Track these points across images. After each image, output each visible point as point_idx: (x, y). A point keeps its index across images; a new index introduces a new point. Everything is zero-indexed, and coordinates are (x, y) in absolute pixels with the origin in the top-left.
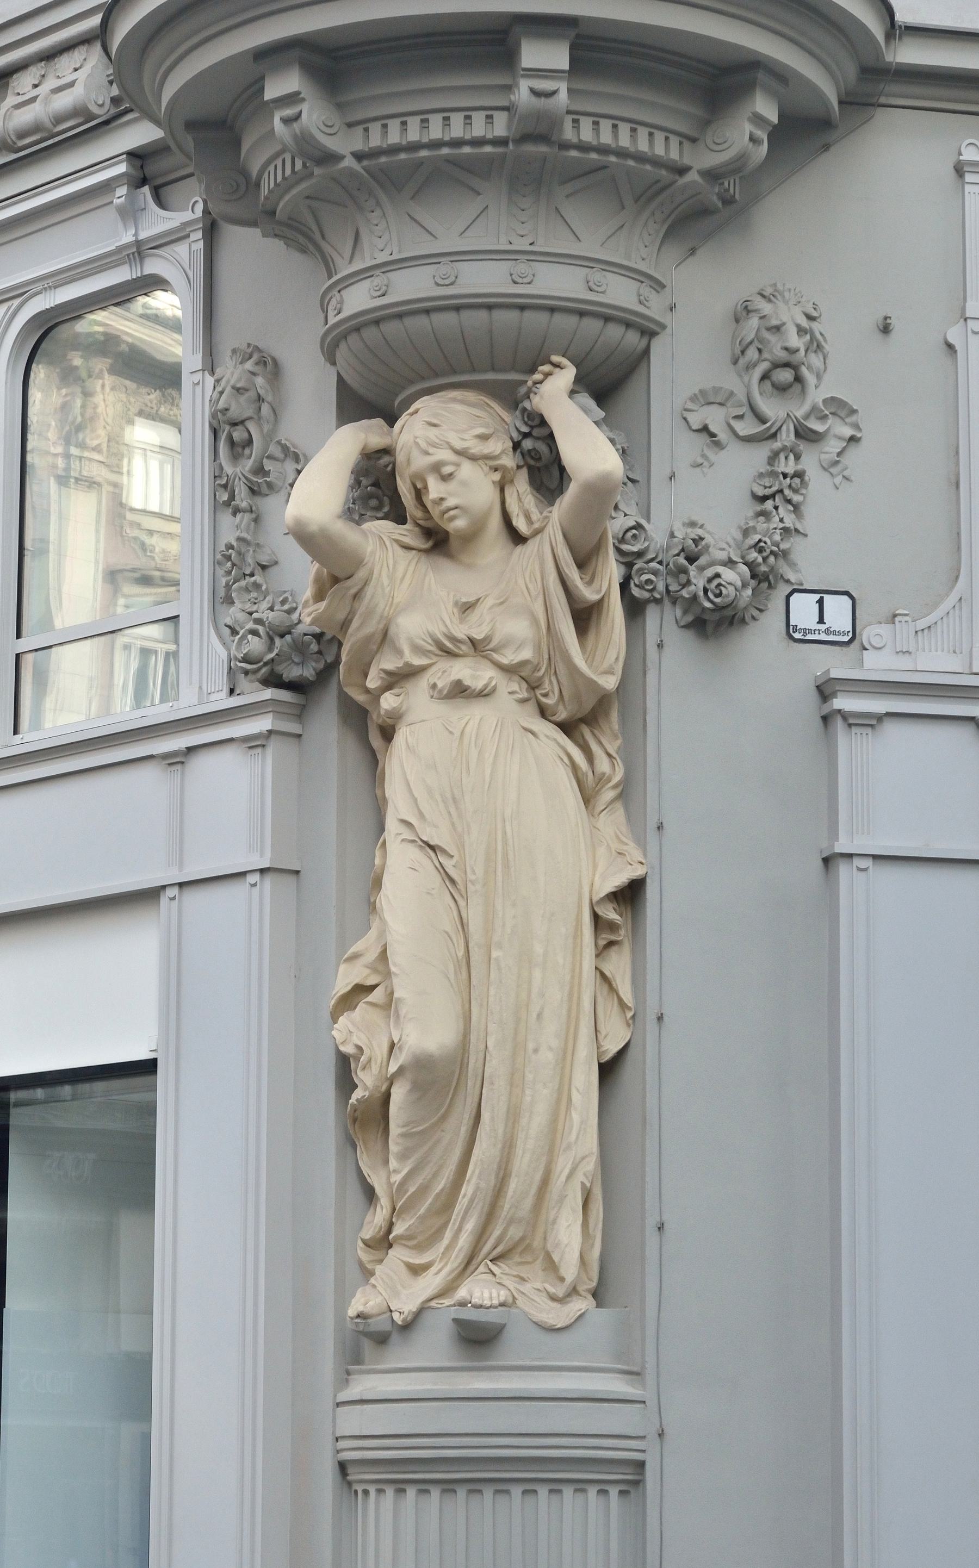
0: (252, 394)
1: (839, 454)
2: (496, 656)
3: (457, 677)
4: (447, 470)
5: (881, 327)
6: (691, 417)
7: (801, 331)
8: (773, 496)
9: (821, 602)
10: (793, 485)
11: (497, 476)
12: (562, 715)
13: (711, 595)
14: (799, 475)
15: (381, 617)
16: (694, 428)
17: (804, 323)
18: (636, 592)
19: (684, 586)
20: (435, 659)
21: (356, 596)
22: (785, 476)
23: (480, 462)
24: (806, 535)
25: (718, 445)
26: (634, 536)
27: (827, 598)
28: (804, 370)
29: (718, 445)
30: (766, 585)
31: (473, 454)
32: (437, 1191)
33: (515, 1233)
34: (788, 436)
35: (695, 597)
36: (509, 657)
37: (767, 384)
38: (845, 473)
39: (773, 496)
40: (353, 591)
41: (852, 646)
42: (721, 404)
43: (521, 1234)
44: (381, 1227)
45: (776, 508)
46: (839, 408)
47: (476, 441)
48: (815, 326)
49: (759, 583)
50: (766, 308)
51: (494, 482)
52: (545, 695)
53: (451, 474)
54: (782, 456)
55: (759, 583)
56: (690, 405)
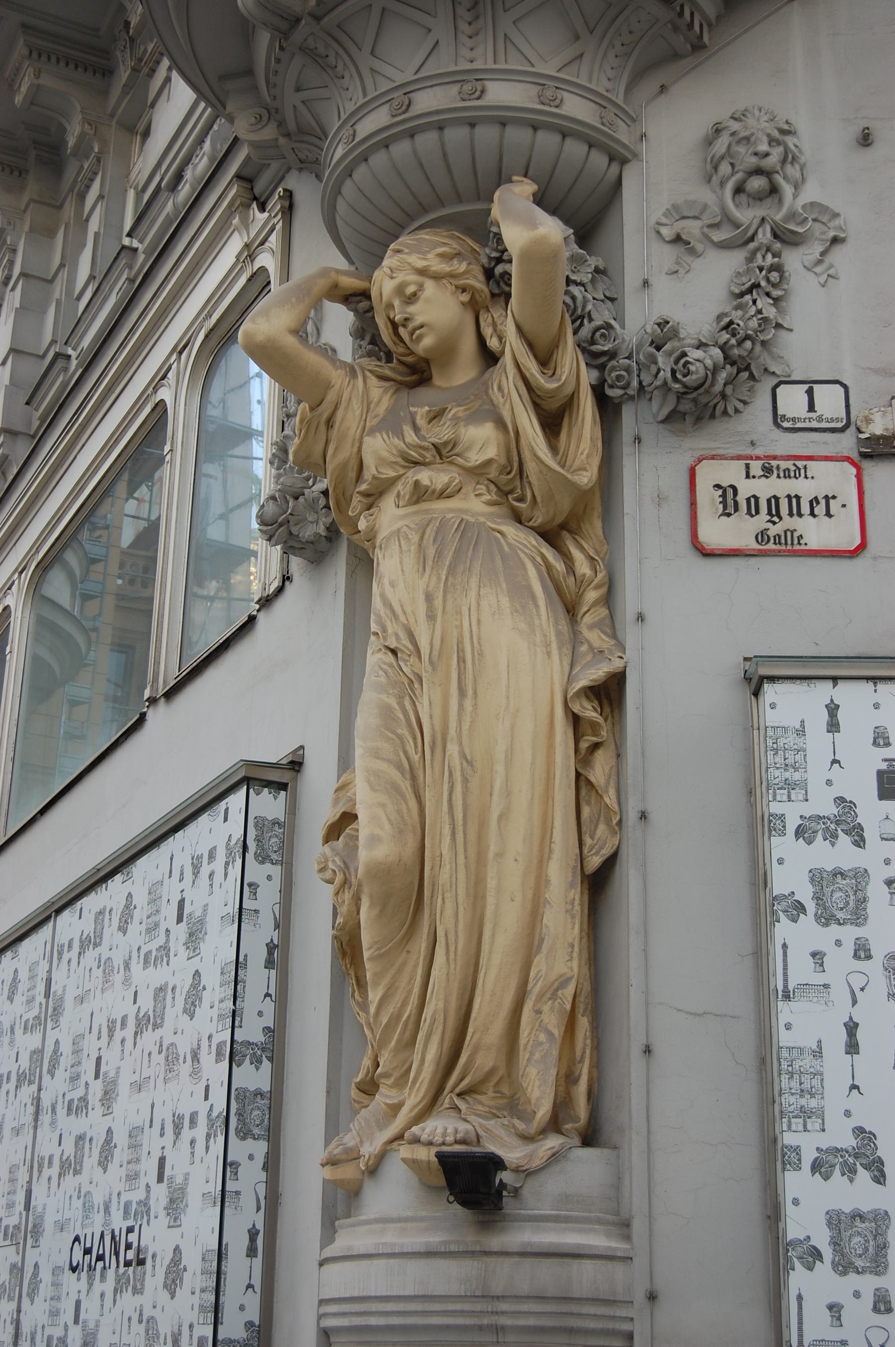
1: (823, 254)
2: (459, 460)
3: (414, 479)
4: (411, 289)
5: (861, 141)
6: (665, 231)
7: (772, 141)
8: (750, 291)
9: (810, 393)
10: (772, 279)
11: (465, 297)
12: (539, 519)
13: (679, 376)
14: (777, 268)
15: (354, 440)
16: (667, 239)
17: (776, 134)
18: (610, 392)
20: (402, 472)
21: (329, 423)
22: (761, 269)
23: (444, 281)
24: (791, 330)
25: (692, 252)
26: (603, 335)
27: (816, 387)
28: (779, 179)
29: (692, 252)
30: (746, 374)
31: (434, 272)
32: (404, 1019)
33: (485, 1061)
34: (764, 235)
36: (475, 458)
37: (743, 198)
38: (832, 272)
39: (750, 291)
40: (325, 416)
41: (848, 431)
42: (696, 218)
43: (491, 1064)
44: (368, 1068)
45: (754, 302)
46: (821, 212)
47: (438, 260)
48: (790, 141)
49: (738, 373)
50: (735, 126)
51: (463, 304)
52: (521, 499)
53: (414, 294)
54: (759, 256)
55: (738, 373)
56: (664, 220)
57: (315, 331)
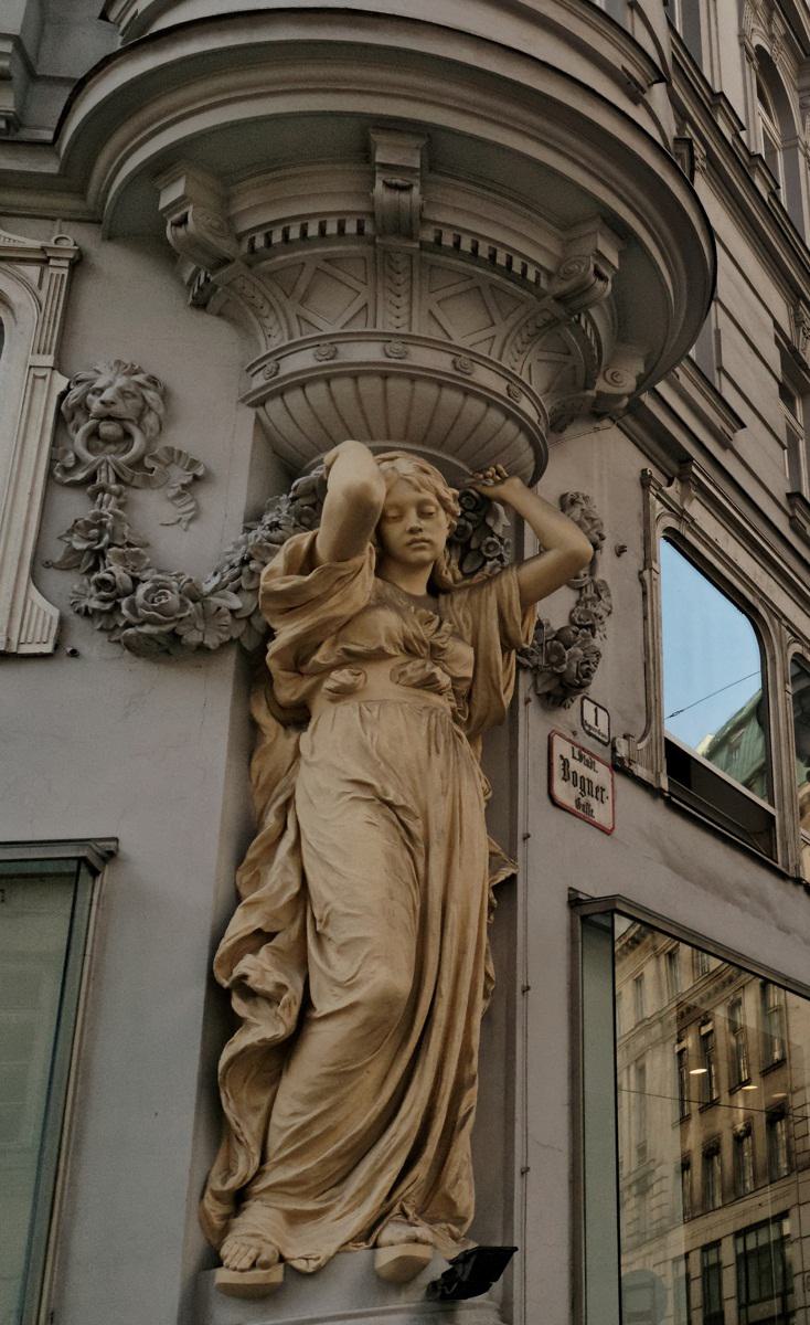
0: (138, 403)
8: (586, 627)
19: (552, 664)
35: (560, 675)
39: (586, 627)
57: (158, 428)
